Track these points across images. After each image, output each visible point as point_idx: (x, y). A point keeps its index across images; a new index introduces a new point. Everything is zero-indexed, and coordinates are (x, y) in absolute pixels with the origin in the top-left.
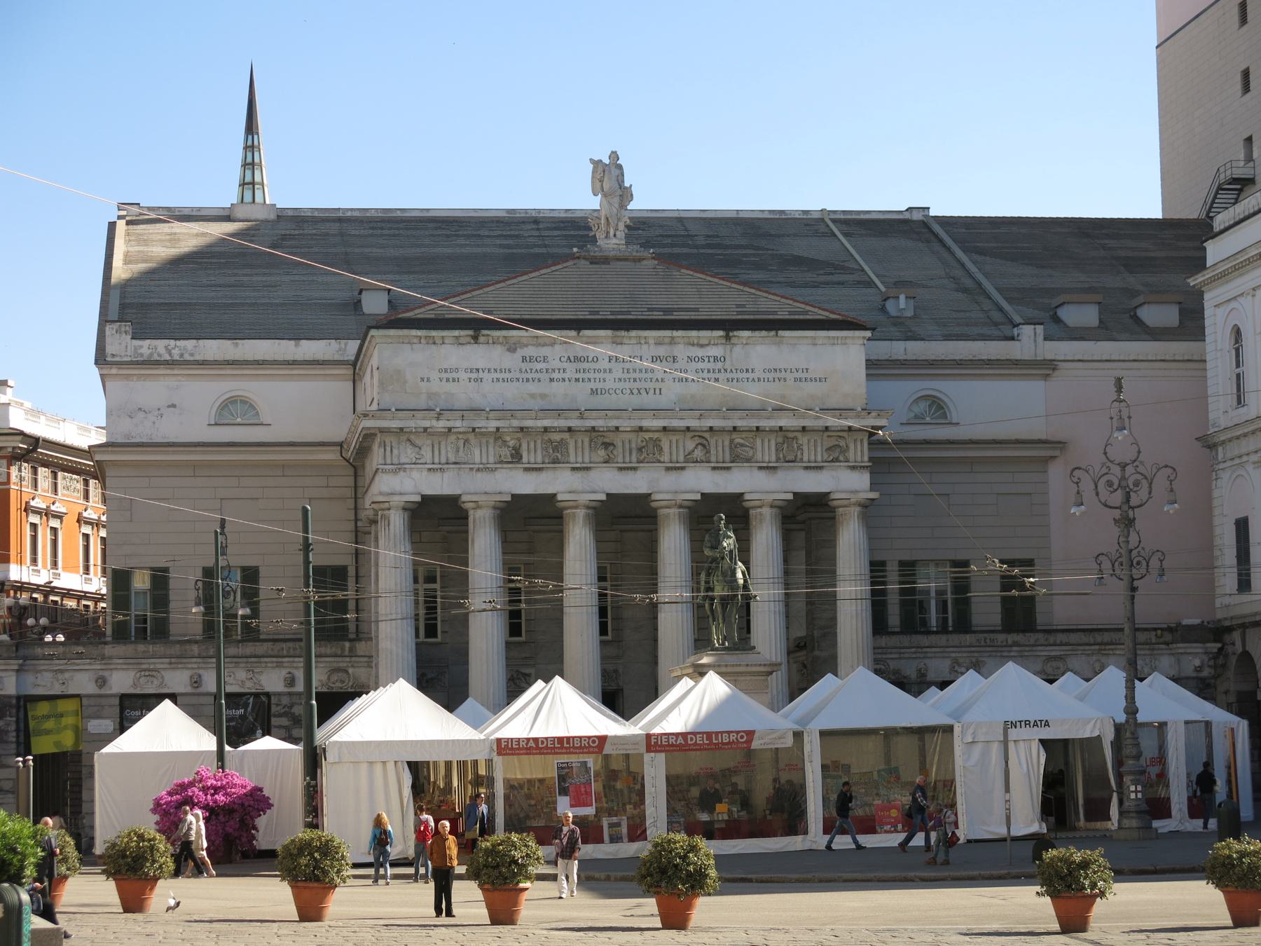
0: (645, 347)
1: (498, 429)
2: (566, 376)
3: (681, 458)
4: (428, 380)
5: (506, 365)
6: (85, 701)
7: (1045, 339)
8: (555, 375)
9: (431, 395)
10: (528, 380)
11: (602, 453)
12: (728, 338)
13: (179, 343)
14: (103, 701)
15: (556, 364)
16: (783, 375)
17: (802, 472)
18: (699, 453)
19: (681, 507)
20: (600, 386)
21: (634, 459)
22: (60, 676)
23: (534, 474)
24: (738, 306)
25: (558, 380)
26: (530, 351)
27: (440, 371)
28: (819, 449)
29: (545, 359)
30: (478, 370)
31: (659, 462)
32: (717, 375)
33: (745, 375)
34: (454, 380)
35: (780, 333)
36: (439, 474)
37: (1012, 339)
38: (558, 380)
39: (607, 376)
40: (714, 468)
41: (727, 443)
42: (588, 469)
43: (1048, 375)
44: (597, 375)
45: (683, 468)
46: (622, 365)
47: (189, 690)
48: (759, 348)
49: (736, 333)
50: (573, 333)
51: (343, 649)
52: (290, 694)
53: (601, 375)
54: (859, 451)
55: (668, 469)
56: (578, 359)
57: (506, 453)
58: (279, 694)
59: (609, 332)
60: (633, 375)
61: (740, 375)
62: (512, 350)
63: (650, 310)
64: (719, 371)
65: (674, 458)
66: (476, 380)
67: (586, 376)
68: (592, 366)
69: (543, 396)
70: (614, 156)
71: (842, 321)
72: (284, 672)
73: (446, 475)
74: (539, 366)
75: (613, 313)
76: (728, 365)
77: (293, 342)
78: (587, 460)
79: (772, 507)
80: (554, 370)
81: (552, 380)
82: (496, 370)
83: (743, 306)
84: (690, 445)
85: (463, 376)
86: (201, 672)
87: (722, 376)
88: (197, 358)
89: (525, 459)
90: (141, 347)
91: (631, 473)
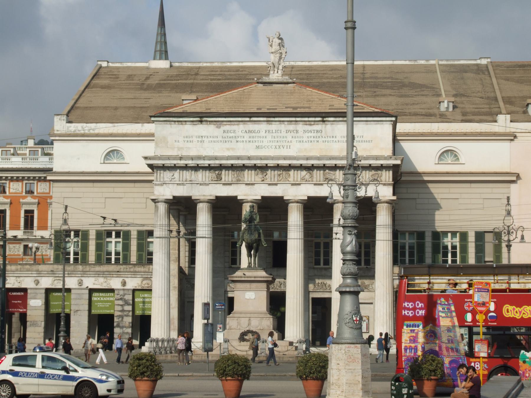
0: (283, 126)
1: (209, 165)
2: (244, 140)
3: (299, 179)
4: (178, 142)
5: (216, 134)
6: (29, 291)
7: (511, 121)
8: (239, 139)
9: (179, 149)
10: (226, 142)
11: (260, 176)
12: (323, 121)
13: (88, 125)
14: (38, 291)
15: (240, 134)
18: (307, 177)
19: (297, 202)
20: (260, 144)
21: (276, 180)
22: (19, 279)
23: (228, 186)
24: (330, 106)
25: (240, 142)
26: (227, 127)
27: (184, 137)
29: (234, 132)
30: (202, 137)
31: (288, 181)
32: (318, 139)
33: (332, 139)
34: (190, 142)
36: (182, 186)
37: (496, 121)
38: (240, 142)
39: (264, 139)
40: (315, 184)
42: (253, 184)
43: (512, 140)
44: (259, 139)
45: (299, 184)
47: (77, 287)
51: (149, 269)
52: (124, 290)
53: (261, 139)
54: (387, 176)
55: (293, 184)
56: (250, 132)
58: (118, 290)
59: (265, 119)
60: (276, 139)
61: (329, 139)
62: (219, 127)
63: (286, 108)
64: (319, 137)
65: (296, 179)
66: (201, 142)
67: (254, 139)
68: (257, 135)
69: (233, 149)
71: (381, 112)
72: (121, 279)
75: (268, 109)
76: (323, 134)
77: (140, 125)
78: (253, 180)
81: (237, 141)
82: (210, 137)
83: (333, 105)
84: (304, 173)
85: (195, 139)
86: (82, 278)
87: (320, 140)
88: (96, 132)
89: (223, 180)
90: (71, 127)
91: (274, 187)
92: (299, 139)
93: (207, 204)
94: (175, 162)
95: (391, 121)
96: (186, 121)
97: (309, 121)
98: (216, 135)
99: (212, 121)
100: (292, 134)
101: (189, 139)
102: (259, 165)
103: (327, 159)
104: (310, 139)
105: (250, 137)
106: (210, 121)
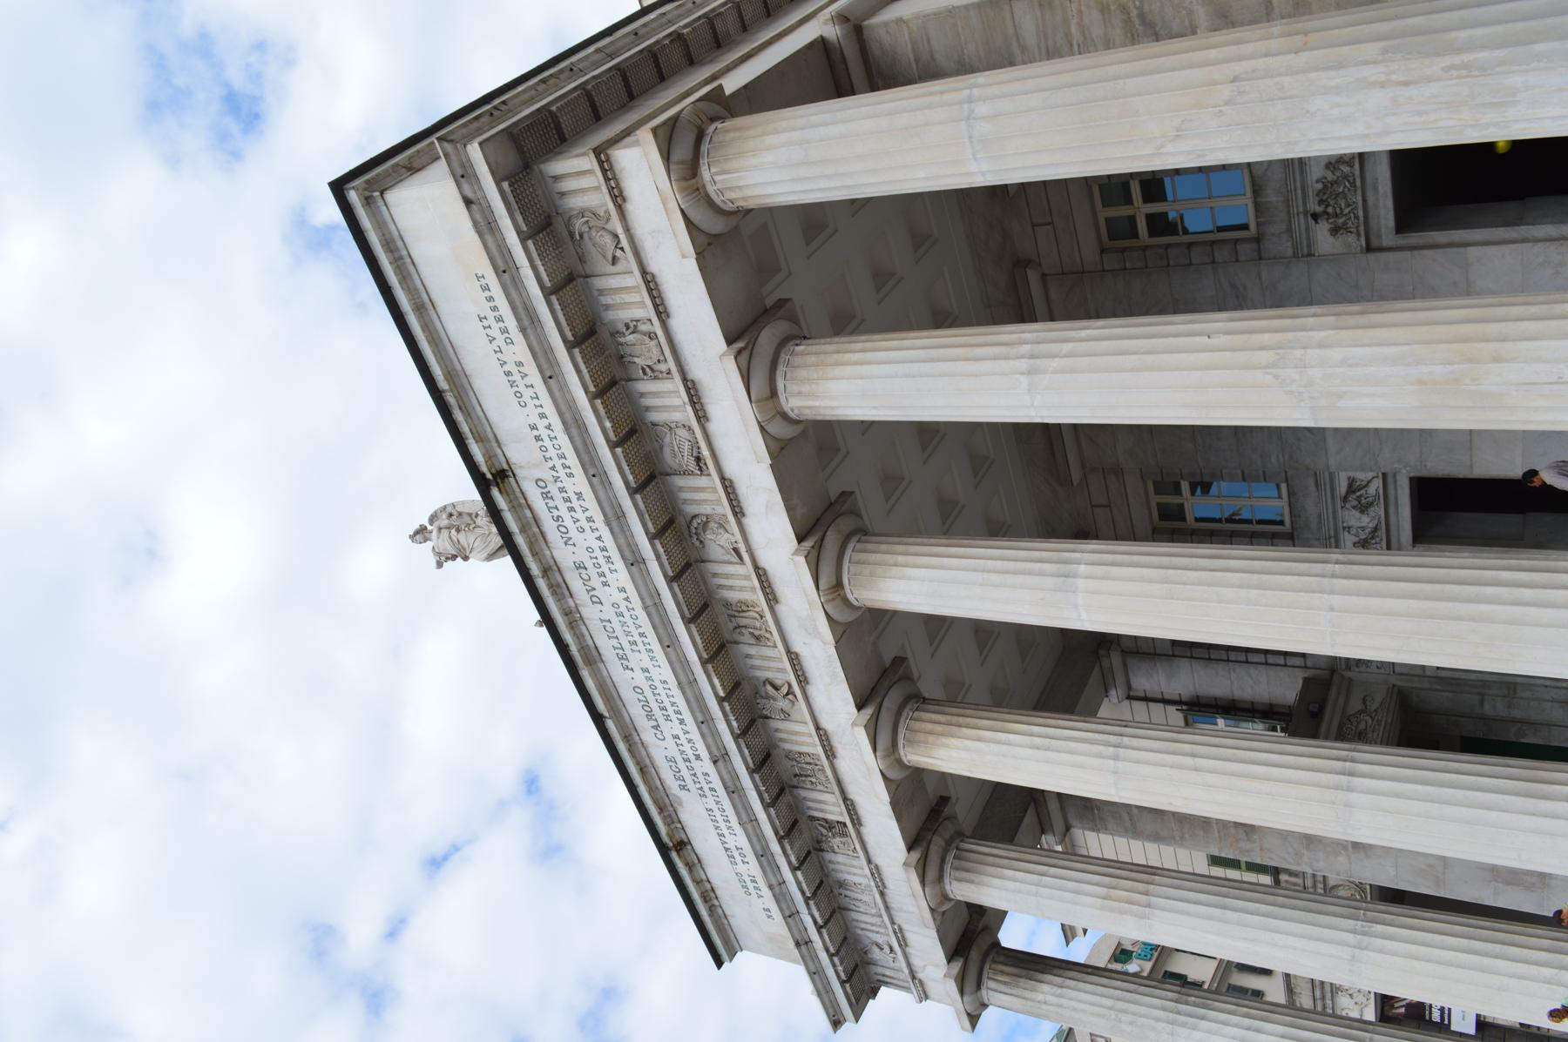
0: (584, 611)
1: (794, 869)
8: (690, 753)
15: (670, 742)
16: (510, 367)
17: (675, 323)
18: (724, 539)
19: (839, 584)
25: (694, 748)
28: (614, 282)
32: (574, 498)
35: (443, 384)
36: (908, 935)
39: (654, 673)
41: (679, 481)
46: (628, 652)
48: (493, 416)
49: (484, 469)
50: (610, 724)
53: (660, 686)
56: (650, 716)
57: (836, 842)
59: (585, 674)
64: (562, 490)
70: (421, 534)
73: (904, 926)
74: (685, 773)
76: (547, 475)
79: (774, 393)
80: (682, 752)
92: (602, 561)
93: (947, 880)
94: (823, 956)
95: (368, 201)
96: (698, 882)
97: (523, 530)
98: (705, 813)
99: (664, 819)
100: (596, 582)
101: (751, 885)
102: (735, 724)
103: (606, 483)
104: (583, 523)
105: (668, 718)
106: (668, 824)
